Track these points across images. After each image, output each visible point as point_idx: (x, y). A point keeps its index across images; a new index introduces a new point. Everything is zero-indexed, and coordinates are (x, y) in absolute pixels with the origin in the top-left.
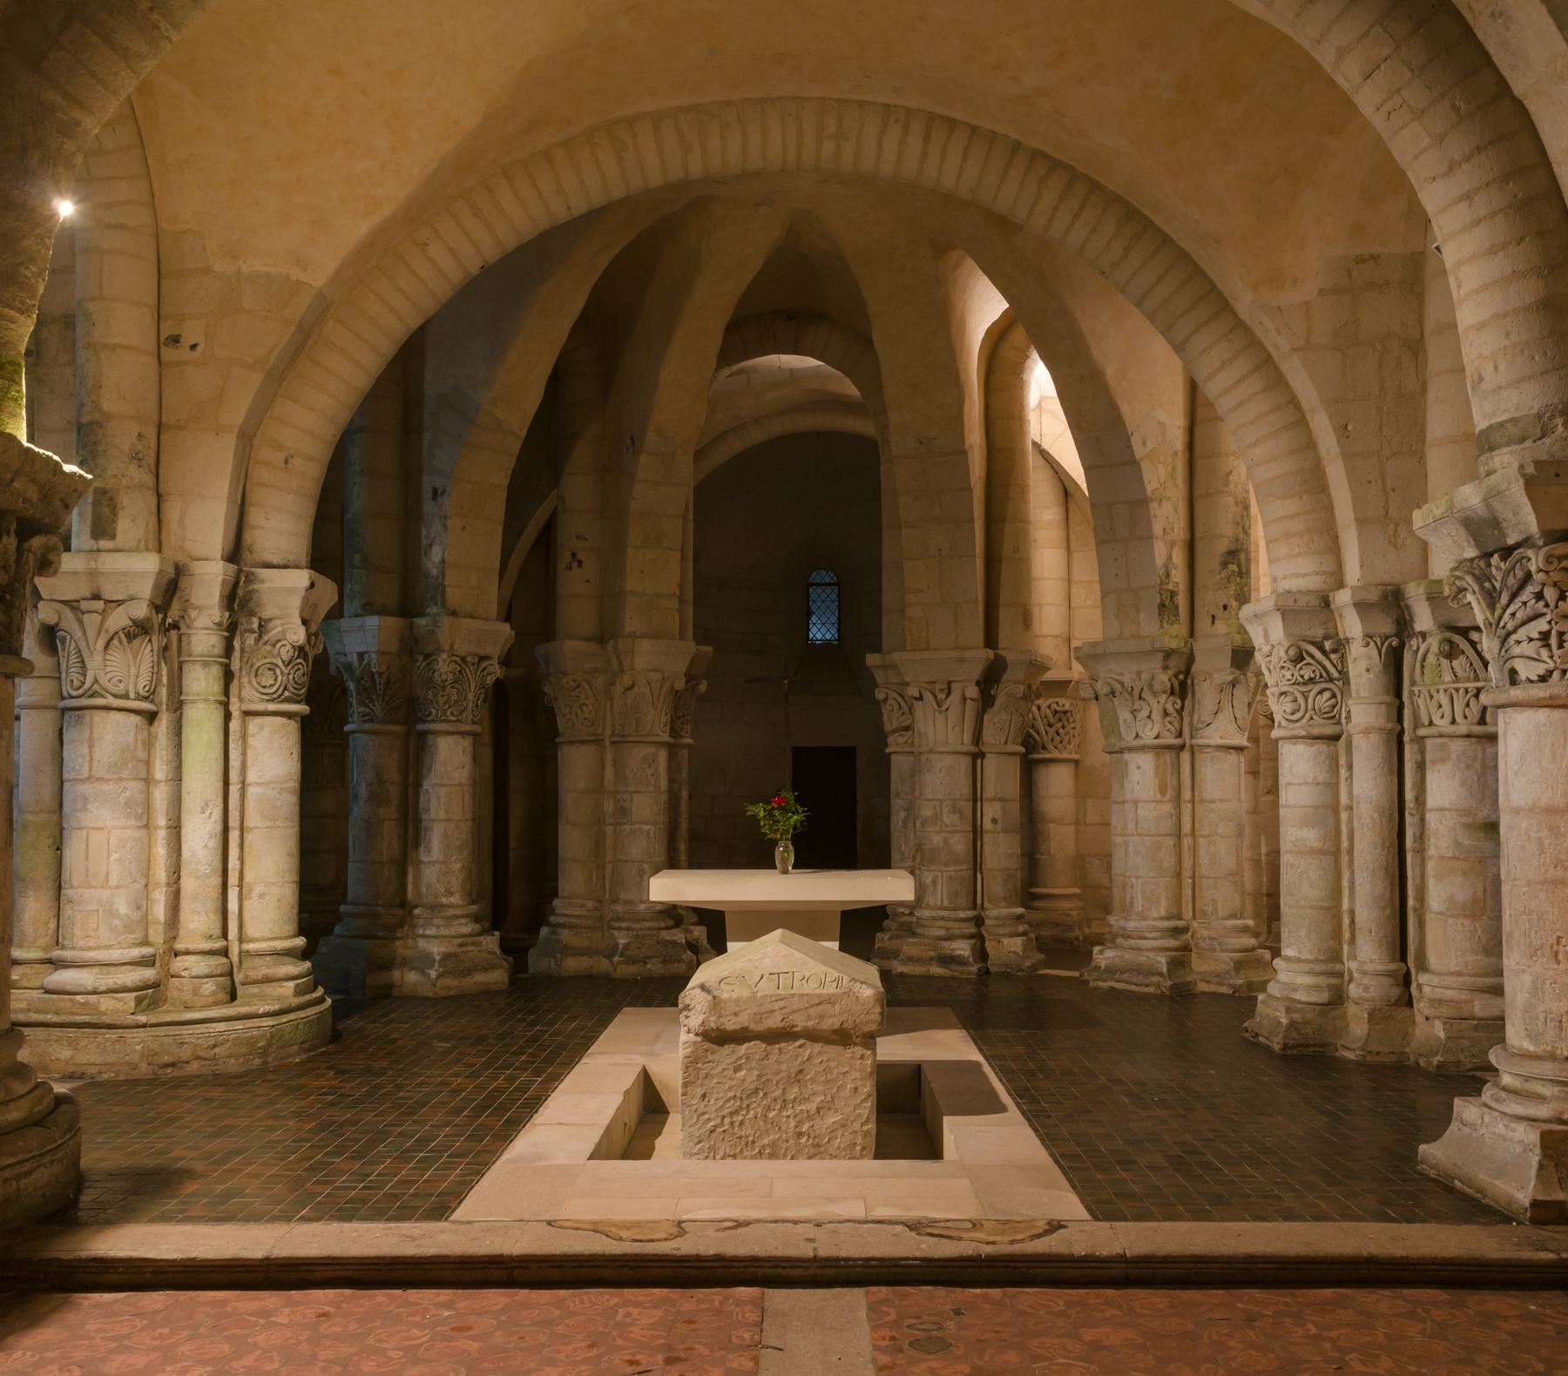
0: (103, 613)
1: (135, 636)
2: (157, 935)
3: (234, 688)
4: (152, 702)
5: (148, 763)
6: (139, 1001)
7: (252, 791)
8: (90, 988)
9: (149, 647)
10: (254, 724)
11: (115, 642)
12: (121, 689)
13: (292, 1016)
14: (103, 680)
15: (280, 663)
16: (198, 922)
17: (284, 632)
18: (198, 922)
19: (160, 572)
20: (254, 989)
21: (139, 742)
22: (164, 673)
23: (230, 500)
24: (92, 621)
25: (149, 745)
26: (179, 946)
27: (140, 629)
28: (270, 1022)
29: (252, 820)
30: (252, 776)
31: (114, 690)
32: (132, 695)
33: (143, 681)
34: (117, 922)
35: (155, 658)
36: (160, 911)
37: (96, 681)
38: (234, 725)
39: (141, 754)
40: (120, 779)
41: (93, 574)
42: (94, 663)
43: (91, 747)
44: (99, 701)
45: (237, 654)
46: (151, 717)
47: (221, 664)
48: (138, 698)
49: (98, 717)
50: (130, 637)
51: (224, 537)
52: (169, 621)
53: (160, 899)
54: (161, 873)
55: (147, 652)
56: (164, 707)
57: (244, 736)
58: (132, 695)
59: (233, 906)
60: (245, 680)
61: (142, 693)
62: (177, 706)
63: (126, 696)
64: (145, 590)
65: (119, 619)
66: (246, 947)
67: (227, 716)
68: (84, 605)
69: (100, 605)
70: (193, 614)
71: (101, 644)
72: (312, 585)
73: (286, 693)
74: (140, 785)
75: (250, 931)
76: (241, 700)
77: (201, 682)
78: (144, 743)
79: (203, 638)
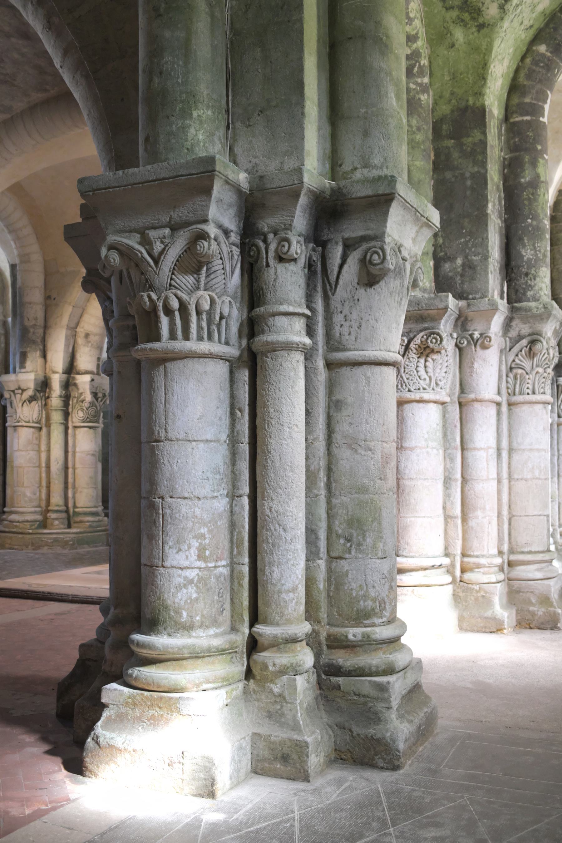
0: (22, 394)
1: (32, 401)
2: (43, 504)
3: (70, 418)
4: (40, 424)
5: (39, 445)
6: (31, 526)
7: (78, 455)
8: (17, 520)
9: (37, 405)
10: (78, 431)
11: (25, 404)
12: (27, 419)
13: (85, 535)
14: (22, 417)
15: (85, 409)
16: (57, 499)
17: (85, 397)
18: (57, 499)
19: (35, 379)
20: (76, 525)
21: (34, 438)
22: (44, 412)
23: (66, 351)
24: (18, 396)
25: (39, 439)
26: (50, 508)
27: (32, 399)
28: (74, 536)
29: (78, 465)
30: (77, 449)
31: (24, 419)
32: (31, 421)
33: (35, 416)
34: (26, 499)
35: (40, 409)
36: (44, 496)
37: (20, 417)
38: (70, 431)
39: (35, 442)
40: (27, 450)
41: (17, 381)
42: (19, 411)
43: (18, 439)
44: (20, 424)
45: (70, 406)
46: (40, 429)
47: (62, 410)
48: (33, 422)
49: (20, 429)
50: (30, 402)
51: (63, 365)
52: (47, 395)
53: (44, 491)
54: (44, 483)
55: (36, 406)
56: (44, 425)
57: (74, 435)
58: (31, 421)
59: (70, 494)
60: (73, 415)
61: (35, 421)
62: (48, 425)
63: (29, 422)
64: (32, 385)
65: (26, 395)
66: (77, 510)
67: (66, 429)
68: (16, 392)
69: (20, 391)
70: (52, 392)
71: (20, 404)
72: (93, 380)
73: (88, 420)
74: (35, 453)
75: (78, 505)
76: (73, 422)
77: (57, 417)
78: (36, 438)
79: (55, 401)
